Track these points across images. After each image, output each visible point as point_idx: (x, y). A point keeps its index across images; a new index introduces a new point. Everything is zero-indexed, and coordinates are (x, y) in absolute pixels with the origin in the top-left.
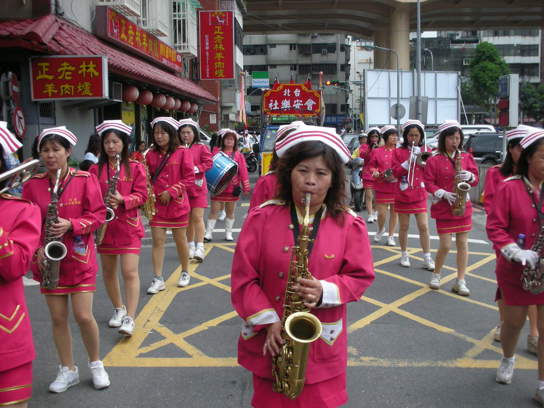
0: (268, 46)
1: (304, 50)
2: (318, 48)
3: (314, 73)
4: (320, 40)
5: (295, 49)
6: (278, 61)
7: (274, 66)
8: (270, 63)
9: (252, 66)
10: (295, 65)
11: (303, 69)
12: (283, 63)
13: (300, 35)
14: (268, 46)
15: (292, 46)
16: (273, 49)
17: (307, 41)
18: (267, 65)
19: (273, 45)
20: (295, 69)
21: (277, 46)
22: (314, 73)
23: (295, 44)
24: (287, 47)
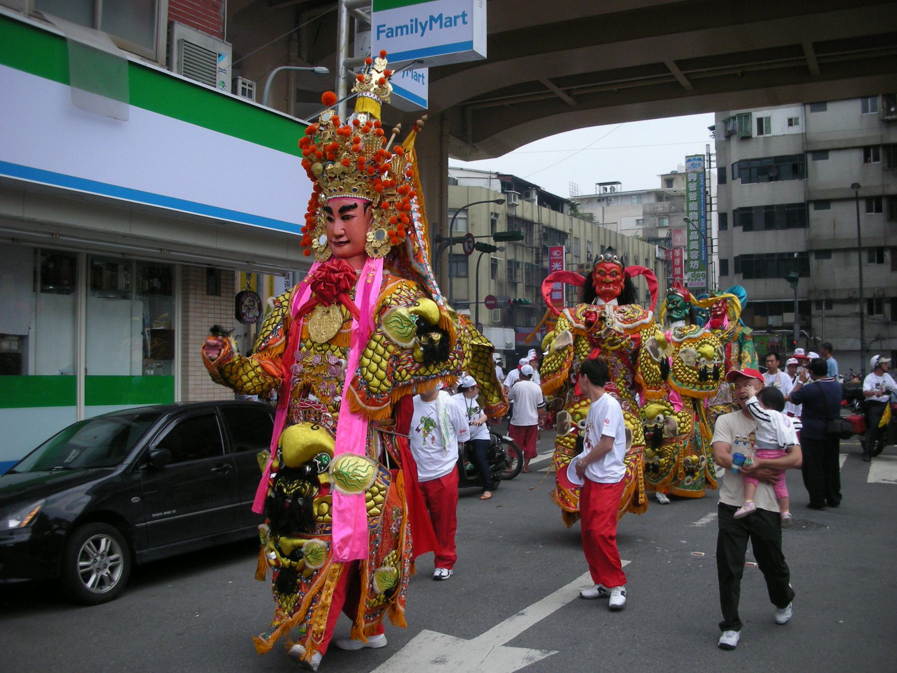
0: (809, 157)
5: (876, 159)
6: (834, 190)
7: (823, 204)
9: (771, 207)
10: (878, 199)
13: (888, 123)
14: (809, 157)
15: (868, 152)
16: (820, 163)
18: (809, 202)
19: (822, 154)
20: (879, 210)
21: (832, 155)
23: (876, 147)
24: (858, 155)
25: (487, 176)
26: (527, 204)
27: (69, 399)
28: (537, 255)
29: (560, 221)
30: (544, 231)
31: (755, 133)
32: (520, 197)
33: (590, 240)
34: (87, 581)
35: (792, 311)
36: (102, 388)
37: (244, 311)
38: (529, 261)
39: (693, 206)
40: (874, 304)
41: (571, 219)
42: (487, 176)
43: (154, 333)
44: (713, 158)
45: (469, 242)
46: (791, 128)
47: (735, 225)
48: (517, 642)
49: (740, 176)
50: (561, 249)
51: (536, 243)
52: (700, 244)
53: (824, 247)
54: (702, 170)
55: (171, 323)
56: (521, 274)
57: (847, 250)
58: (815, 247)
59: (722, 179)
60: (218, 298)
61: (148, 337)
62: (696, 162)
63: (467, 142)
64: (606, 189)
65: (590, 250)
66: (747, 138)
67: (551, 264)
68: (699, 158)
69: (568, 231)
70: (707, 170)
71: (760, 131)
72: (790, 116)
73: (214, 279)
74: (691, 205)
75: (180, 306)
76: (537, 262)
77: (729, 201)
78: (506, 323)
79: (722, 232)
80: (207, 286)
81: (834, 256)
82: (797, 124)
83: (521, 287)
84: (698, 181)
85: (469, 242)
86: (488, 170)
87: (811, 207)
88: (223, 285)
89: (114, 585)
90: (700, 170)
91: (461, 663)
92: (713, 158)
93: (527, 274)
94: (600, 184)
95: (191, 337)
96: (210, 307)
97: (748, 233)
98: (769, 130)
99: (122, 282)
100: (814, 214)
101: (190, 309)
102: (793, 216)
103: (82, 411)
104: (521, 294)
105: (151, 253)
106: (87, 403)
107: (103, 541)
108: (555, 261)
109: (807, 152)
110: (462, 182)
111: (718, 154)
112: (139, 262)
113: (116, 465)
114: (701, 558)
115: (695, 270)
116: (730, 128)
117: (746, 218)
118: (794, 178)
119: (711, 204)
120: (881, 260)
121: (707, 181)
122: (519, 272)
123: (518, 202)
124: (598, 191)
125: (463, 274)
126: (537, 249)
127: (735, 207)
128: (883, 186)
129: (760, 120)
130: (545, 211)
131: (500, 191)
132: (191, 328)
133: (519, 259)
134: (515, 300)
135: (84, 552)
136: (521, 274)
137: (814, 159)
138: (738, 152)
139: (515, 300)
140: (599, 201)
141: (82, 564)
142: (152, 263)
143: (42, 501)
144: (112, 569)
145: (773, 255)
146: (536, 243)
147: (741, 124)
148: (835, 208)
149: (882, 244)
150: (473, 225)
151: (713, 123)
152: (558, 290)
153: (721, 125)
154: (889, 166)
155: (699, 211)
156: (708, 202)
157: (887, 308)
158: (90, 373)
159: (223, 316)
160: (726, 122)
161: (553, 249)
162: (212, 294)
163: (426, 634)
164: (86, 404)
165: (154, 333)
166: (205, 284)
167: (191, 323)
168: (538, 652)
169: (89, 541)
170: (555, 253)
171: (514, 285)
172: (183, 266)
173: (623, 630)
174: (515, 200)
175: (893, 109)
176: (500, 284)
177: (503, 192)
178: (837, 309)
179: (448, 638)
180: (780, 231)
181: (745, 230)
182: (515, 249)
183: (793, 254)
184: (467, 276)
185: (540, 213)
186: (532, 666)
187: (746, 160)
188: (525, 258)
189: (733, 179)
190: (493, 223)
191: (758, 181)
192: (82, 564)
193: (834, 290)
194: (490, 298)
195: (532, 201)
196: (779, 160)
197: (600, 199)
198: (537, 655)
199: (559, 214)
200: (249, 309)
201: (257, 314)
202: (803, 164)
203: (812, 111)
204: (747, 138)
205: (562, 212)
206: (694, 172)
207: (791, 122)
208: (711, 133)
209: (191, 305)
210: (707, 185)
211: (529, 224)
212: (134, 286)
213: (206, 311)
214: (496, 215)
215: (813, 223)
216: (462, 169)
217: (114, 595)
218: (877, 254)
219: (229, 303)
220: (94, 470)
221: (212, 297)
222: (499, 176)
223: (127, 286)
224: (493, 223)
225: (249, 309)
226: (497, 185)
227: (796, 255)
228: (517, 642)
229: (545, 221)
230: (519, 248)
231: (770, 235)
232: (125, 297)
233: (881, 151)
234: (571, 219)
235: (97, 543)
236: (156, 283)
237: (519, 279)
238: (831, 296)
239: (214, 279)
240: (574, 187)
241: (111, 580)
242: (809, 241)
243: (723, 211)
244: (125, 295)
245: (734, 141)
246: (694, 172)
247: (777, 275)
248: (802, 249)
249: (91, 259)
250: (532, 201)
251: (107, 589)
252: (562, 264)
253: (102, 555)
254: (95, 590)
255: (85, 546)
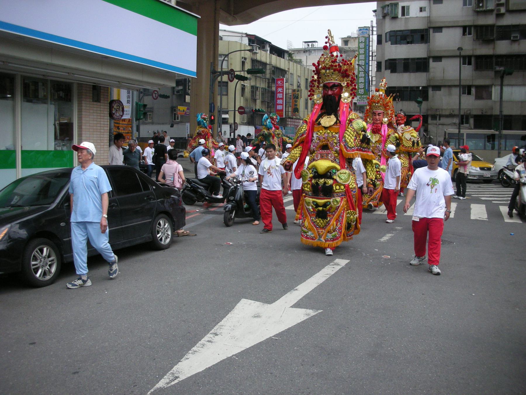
1: (483, 34)
2: (505, 33)
3: (498, 69)
4: (509, 20)
5: (470, 34)
6: (445, 51)
7: (438, 59)
8: (433, 54)
9: (408, 59)
10: (470, 57)
11: (481, 63)
12: (451, 54)
15: (466, 29)
16: (437, 35)
17: (490, 20)
18: (430, 57)
19: (439, 29)
20: (470, 64)
21: (444, 30)
22: (498, 69)
23: (470, 27)
24: (459, 31)
25: (240, 35)
26: (263, 52)
27: (13, 165)
28: (269, 83)
29: (282, 63)
30: (273, 69)
31: (400, 15)
32: (259, 49)
33: (299, 75)
34: (36, 273)
35: (417, 120)
36: (31, 158)
37: (114, 112)
38: (264, 87)
39: (362, 57)
40: (464, 119)
41: (289, 62)
42: (240, 35)
43: (61, 125)
44: (375, 29)
45: (232, 74)
46: (421, 13)
47: (386, 69)
48: (297, 305)
49: (390, 40)
50: (283, 80)
51: (268, 76)
52: (365, 80)
53: (437, 84)
54: (367, 36)
55: (71, 119)
56: (259, 94)
57: (450, 86)
58: (432, 84)
59: (379, 42)
60: (99, 104)
61: (57, 127)
62: (364, 31)
63: (230, 14)
64: (309, 45)
65: (299, 81)
66: (395, 18)
67: (277, 89)
68: (367, 28)
69: (287, 69)
70: (371, 36)
71: (403, 14)
72: (421, 6)
73: (97, 92)
74: (360, 56)
75: (77, 108)
76: (269, 87)
77: (383, 54)
78: (250, 123)
79: (379, 73)
80: (93, 97)
81: (442, 89)
82: (425, 11)
83: (258, 102)
84: (365, 42)
85: (232, 74)
86: (241, 31)
87: (431, 60)
88: (102, 96)
89: (52, 275)
90: (367, 36)
91: (269, 317)
92: (375, 29)
93: (263, 94)
94: (305, 42)
95: (83, 127)
96: (95, 109)
97: (393, 74)
98: (408, 14)
99: (41, 94)
100: (432, 64)
101: (83, 110)
102: (420, 65)
103: (20, 172)
104: (258, 106)
105: (61, 76)
106: (23, 167)
107: (45, 249)
108: (279, 87)
109: (430, 28)
110: (225, 38)
111: (377, 27)
112: (52, 81)
113: (50, 204)
114: (389, 259)
115: (362, 95)
116: (385, 12)
117: (393, 65)
118: (421, 43)
119: (372, 56)
120: (469, 93)
121: (371, 43)
122: (258, 93)
123: (258, 51)
124: (305, 46)
125: (224, 93)
126: (268, 79)
127: (386, 59)
128: (473, 50)
129: (403, 8)
130: (274, 57)
131: (248, 44)
132: (83, 122)
133: (258, 85)
134: (256, 109)
135: (34, 256)
136: (259, 94)
137: (433, 32)
138: (389, 26)
139: (256, 109)
140: (304, 52)
141: (33, 263)
142: (58, 81)
143: (9, 226)
144: (50, 266)
145: (407, 87)
146: (268, 76)
147: (392, 10)
148: (444, 61)
149: (471, 84)
150: (231, 64)
151: (375, 8)
152: (280, 104)
153: (380, 9)
154: (477, 38)
155: (365, 60)
156: (371, 54)
157: (472, 121)
158: (23, 149)
159: (102, 115)
160: (383, 8)
161: (278, 80)
162: (96, 101)
163: (243, 301)
164: (22, 167)
165: (61, 125)
166: (91, 95)
167: (83, 119)
168: (311, 311)
169: (37, 249)
170: (279, 82)
171: (255, 100)
172: (78, 84)
173: (356, 298)
174: (256, 50)
175: (481, 5)
176: (246, 100)
177: (249, 45)
178: (443, 120)
179: (258, 303)
180: (412, 75)
181: (392, 72)
182: (256, 79)
183: (419, 87)
184: (227, 95)
185: (270, 58)
186: (310, 319)
187: (394, 31)
188: (262, 85)
189: (386, 42)
190: (243, 63)
191: (400, 44)
192: (33, 263)
193: (442, 109)
194: (241, 108)
195: (266, 51)
196: (414, 32)
197: (305, 51)
198: (312, 313)
199: (282, 59)
200: (117, 111)
201: (121, 114)
202: (427, 35)
203: (434, 3)
204: (395, 18)
205: (284, 58)
206: (363, 37)
207: (421, 10)
208: (374, 14)
209: (83, 108)
210: (371, 45)
211: (265, 64)
212: (49, 96)
213: (92, 111)
214: (245, 59)
215: (431, 70)
216: (225, 31)
217: (52, 281)
218: (467, 89)
219: (105, 107)
220: (36, 207)
221: (95, 103)
222: (247, 35)
223: (45, 96)
224: (243, 63)
225: (117, 111)
226: (246, 41)
227: (420, 88)
228: (297, 305)
229: (274, 63)
230: (258, 79)
231: (406, 75)
232: (45, 103)
233: (472, 29)
234: (289, 62)
235: (42, 251)
236: (62, 94)
237: (257, 97)
238: (441, 113)
239: (97, 92)
240: (289, 43)
241: (50, 272)
242: (429, 80)
243: (379, 61)
244: (44, 101)
245: (388, 19)
246: (363, 37)
247: (410, 99)
248: (424, 85)
249: (24, 78)
250: (266, 51)
251: (48, 277)
252: (283, 89)
253: (45, 258)
254: (41, 279)
255: (35, 253)
